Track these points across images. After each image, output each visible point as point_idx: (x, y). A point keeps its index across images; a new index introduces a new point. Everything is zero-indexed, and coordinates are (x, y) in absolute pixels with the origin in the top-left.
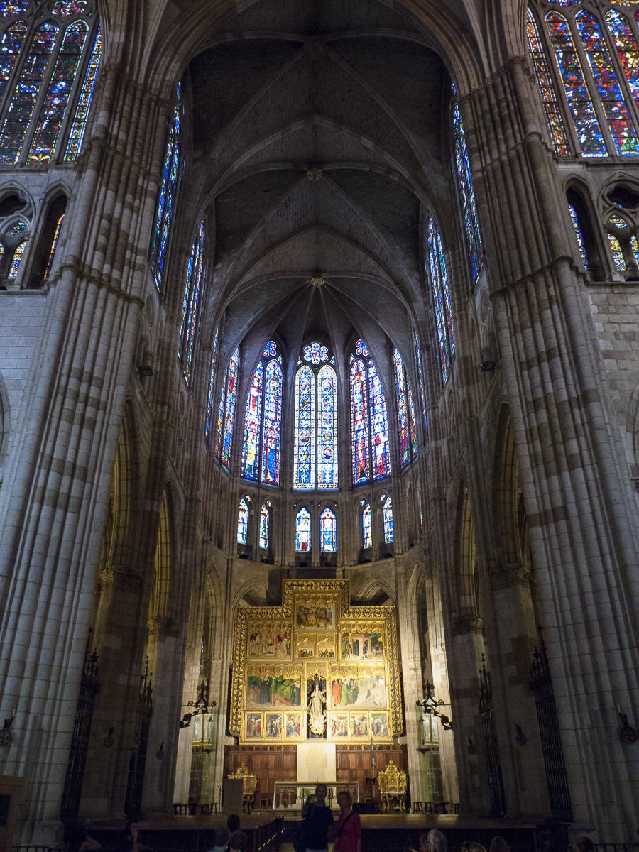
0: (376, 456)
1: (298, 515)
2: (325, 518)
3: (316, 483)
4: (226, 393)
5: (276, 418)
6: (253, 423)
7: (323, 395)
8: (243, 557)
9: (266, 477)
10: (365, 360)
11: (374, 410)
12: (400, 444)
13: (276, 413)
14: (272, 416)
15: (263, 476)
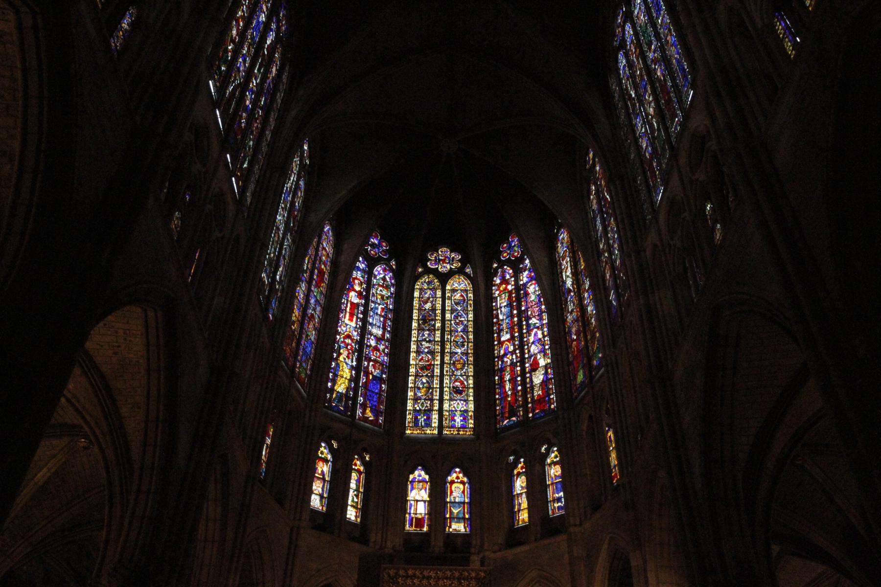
0: (532, 387)
1: (411, 477)
2: (452, 482)
3: (441, 427)
4: (309, 283)
5: (383, 335)
6: (348, 337)
7: (453, 311)
9: (364, 413)
11: (528, 325)
12: (570, 364)
13: (384, 329)
14: (378, 332)
15: (359, 412)
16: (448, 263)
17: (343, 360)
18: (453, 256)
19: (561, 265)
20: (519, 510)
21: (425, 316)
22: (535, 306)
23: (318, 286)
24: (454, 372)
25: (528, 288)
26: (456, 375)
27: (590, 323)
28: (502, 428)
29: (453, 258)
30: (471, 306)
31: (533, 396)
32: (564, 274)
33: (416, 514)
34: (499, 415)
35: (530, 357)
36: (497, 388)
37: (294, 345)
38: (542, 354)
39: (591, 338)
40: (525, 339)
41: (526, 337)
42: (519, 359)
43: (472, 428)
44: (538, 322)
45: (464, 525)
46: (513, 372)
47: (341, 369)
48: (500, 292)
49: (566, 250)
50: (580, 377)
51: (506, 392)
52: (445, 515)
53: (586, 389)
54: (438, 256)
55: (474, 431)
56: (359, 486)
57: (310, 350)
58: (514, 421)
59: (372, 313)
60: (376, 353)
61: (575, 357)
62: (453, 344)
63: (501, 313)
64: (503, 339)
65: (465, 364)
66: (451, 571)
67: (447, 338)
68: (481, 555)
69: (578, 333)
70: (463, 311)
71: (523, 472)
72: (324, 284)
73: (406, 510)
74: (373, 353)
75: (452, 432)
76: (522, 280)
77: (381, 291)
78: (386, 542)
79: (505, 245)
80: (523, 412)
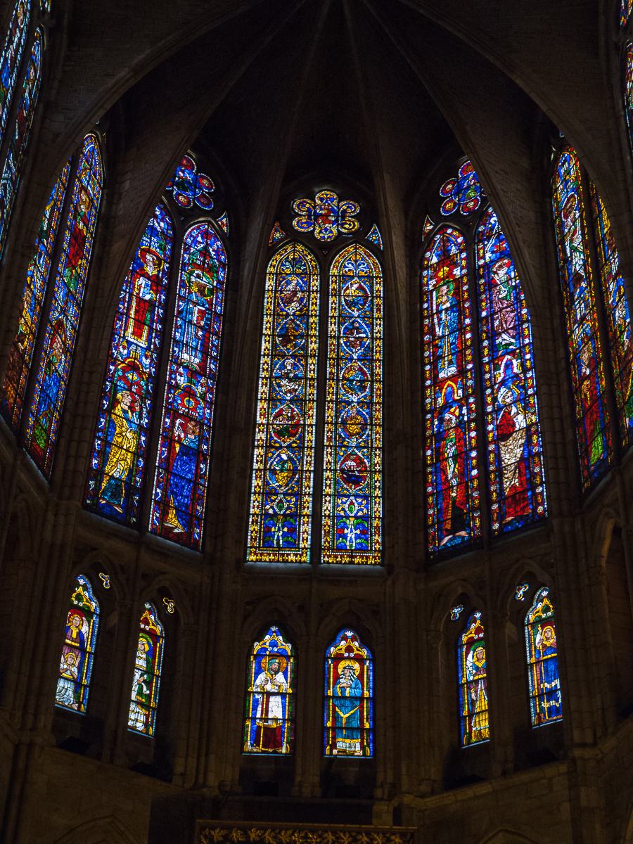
0: (500, 471)
1: (257, 647)
2: (339, 658)
3: (316, 549)
4: (54, 257)
5: (203, 364)
6: (133, 367)
7: (342, 318)
8: (74, 746)
10: (470, 226)
11: (493, 348)
12: (576, 423)
13: (205, 353)
15: (153, 516)
16: (333, 223)
17: (121, 413)
18: (345, 207)
19: (562, 225)
20: (471, 715)
21: (288, 328)
22: (509, 309)
23: (71, 264)
24: (344, 440)
25: (495, 273)
26: (347, 447)
27: (617, 342)
28: (439, 551)
29: (345, 211)
30: (378, 310)
31: (502, 489)
32: (567, 243)
33: (266, 720)
34: (433, 526)
35: (496, 411)
36: (431, 473)
37: (22, 380)
38: (520, 406)
39: (621, 372)
40: (487, 376)
41: (490, 372)
42: (473, 415)
43: (379, 551)
44: (513, 341)
45: (362, 743)
46: (460, 439)
47: (118, 430)
48: (438, 282)
49: (572, 196)
50: (597, 450)
51: (447, 481)
52: (323, 723)
53: (609, 475)
54: (314, 207)
55: (383, 557)
56: (154, 663)
57: (57, 392)
58: (463, 537)
59: (180, 322)
60: (189, 401)
61: (586, 411)
62: (343, 385)
63: (439, 324)
64: (442, 375)
65: (366, 424)
66: (334, 833)
67: (331, 373)
68: (395, 803)
69: (593, 363)
70: (363, 319)
71: (479, 639)
72: (84, 261)
73: (246, 711)
74: (182, 401)
75: (339, 559)
76: (484, 257)
77: (198, 276)
78: (205, 774)
79: (450, 186)
80: (481, 521)
